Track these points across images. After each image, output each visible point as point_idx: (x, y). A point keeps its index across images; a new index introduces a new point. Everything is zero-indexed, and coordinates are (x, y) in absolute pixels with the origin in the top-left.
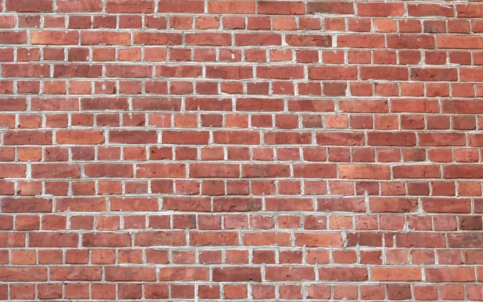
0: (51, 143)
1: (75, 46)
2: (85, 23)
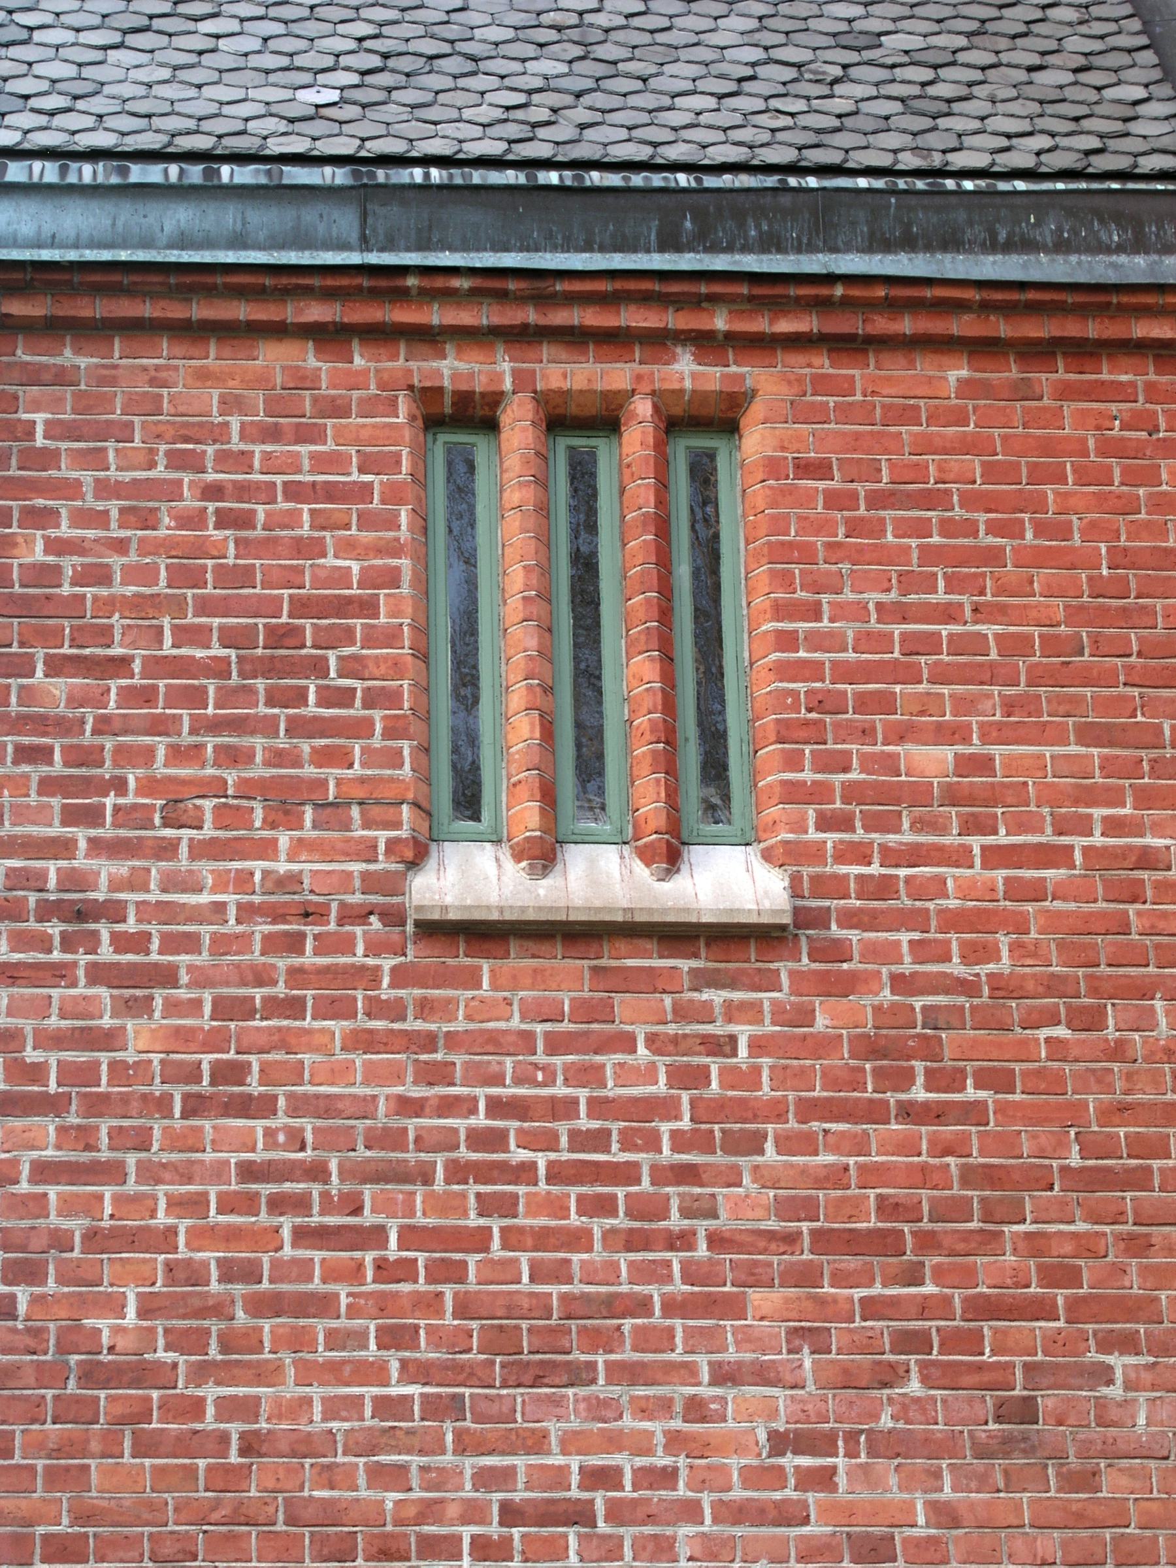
0: (175, 1249)
1: (224, 1056)
2: (245, 1009)
